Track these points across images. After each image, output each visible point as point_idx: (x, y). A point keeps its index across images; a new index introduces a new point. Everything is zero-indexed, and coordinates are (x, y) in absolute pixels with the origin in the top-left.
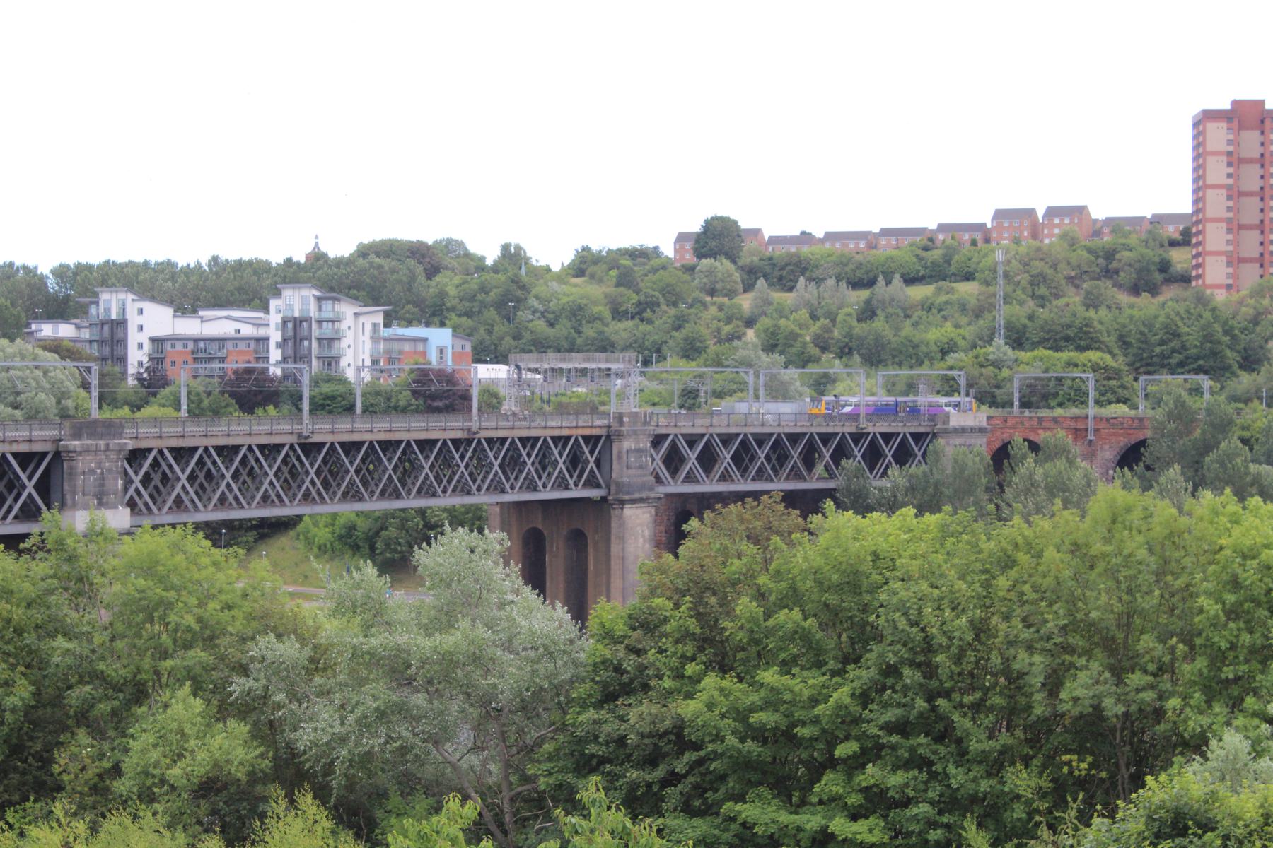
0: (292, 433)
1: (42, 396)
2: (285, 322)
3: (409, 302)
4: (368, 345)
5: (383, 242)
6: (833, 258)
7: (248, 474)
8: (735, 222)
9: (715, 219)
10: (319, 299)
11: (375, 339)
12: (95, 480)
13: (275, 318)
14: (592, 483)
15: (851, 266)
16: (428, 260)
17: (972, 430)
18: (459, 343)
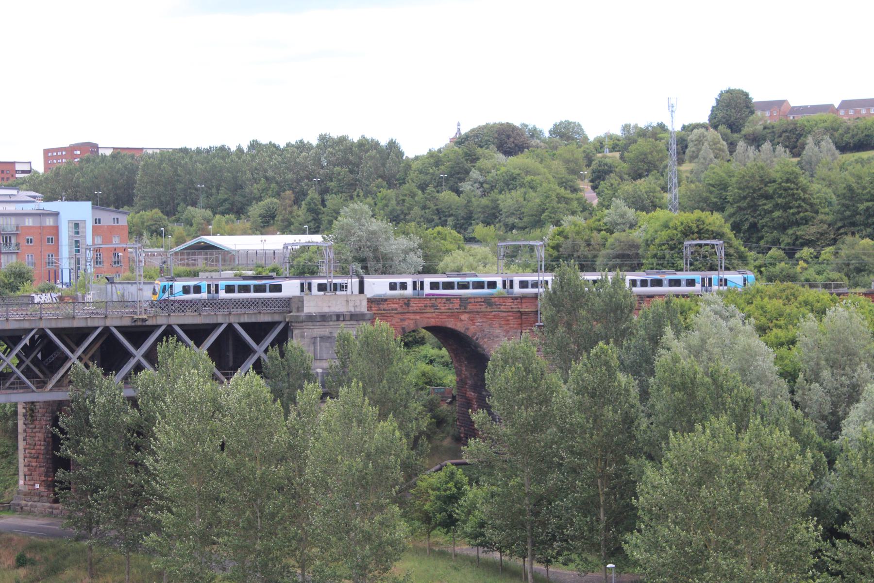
6: (826, 124)
9: (730, 92)
15: (840, 131)
16: (512, 140)
17: (339, 317)
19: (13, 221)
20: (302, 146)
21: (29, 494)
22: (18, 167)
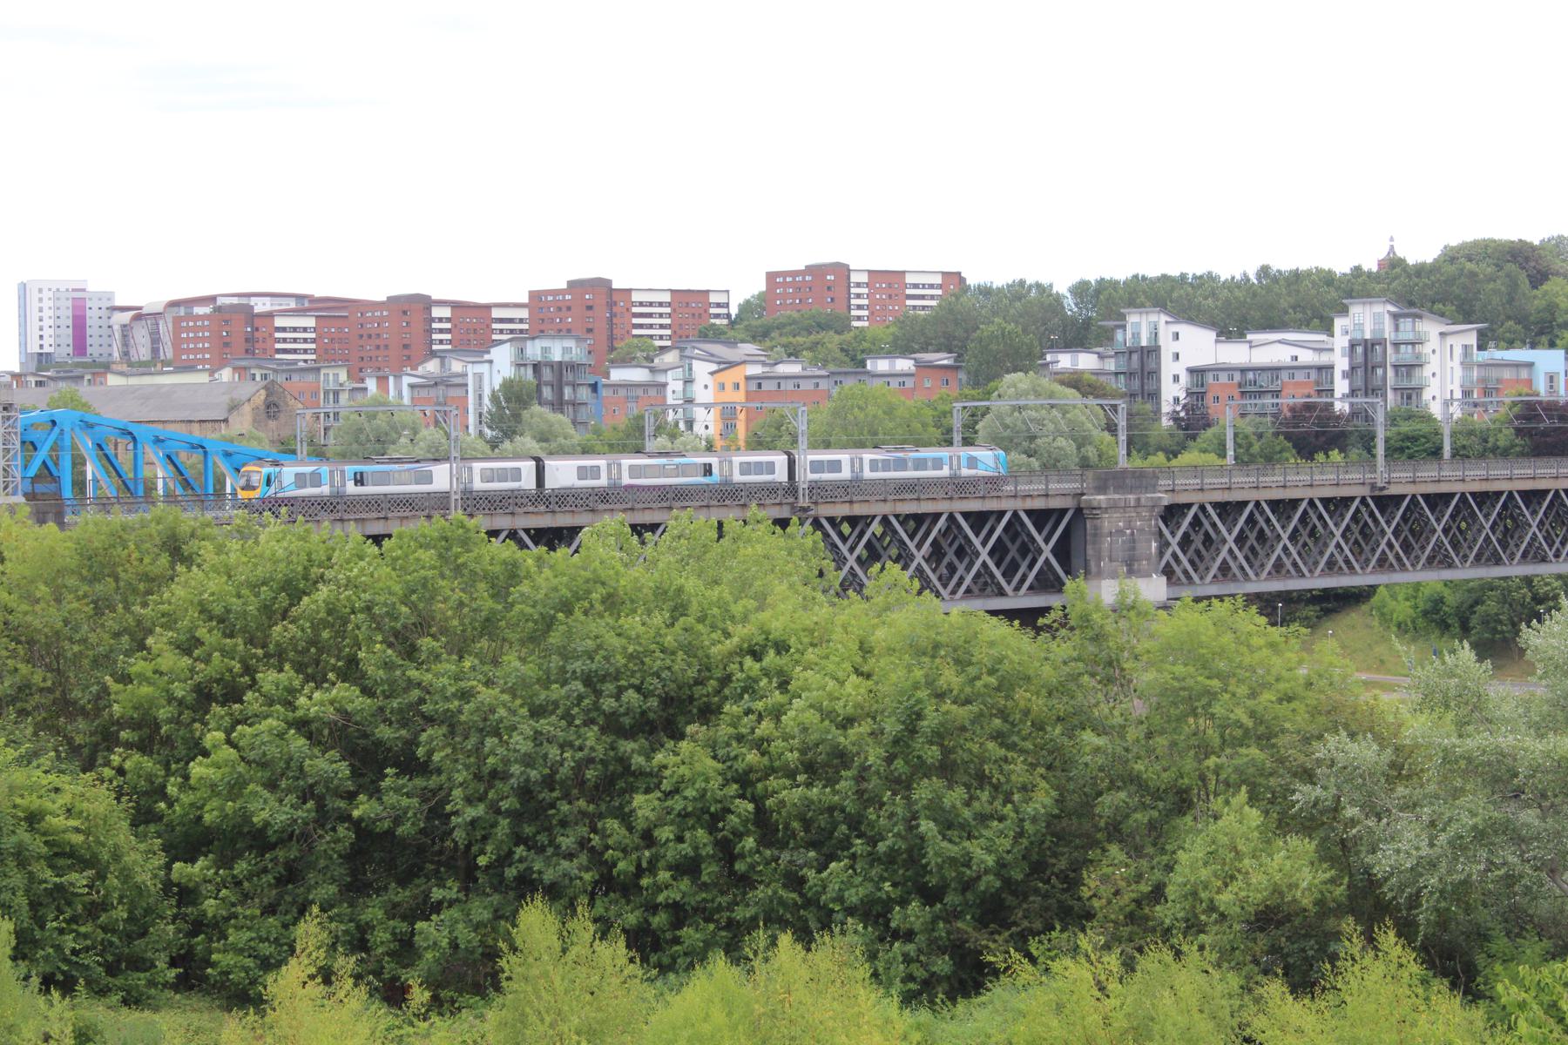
0: (1363, 484)
1: (1061, 442)
2: (1353, 346)
3: (1509, 318)
4: (1458, 372)
5: (1476, 244)
7: (1309, 535)
10: (1395, 317)
11: (1466, 364)
12: (1123, 542)
13: (1340, 341)
22: (713, 298)
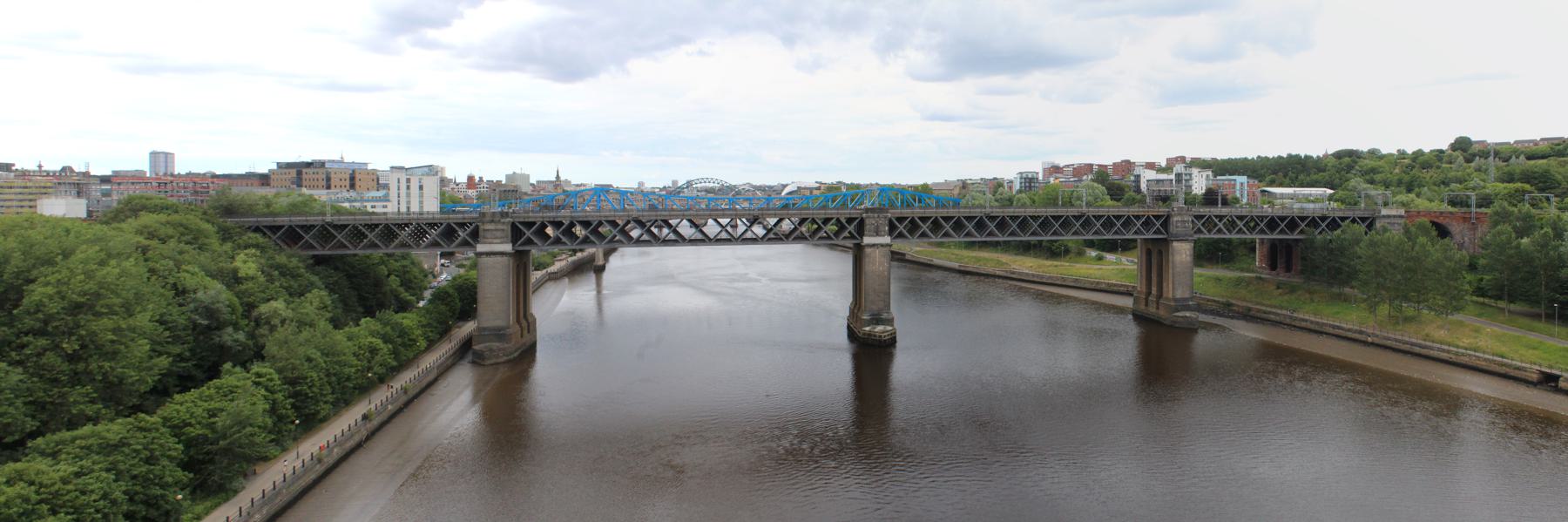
4: (1204, 182)
5: (1342, 151)
8: (1469, 139)
14: (1158, 232)
17: (1394, 216)
18: (1251, 181)
19: (1222, 182)
20: (1280, 157)
21: (1261, 267)
